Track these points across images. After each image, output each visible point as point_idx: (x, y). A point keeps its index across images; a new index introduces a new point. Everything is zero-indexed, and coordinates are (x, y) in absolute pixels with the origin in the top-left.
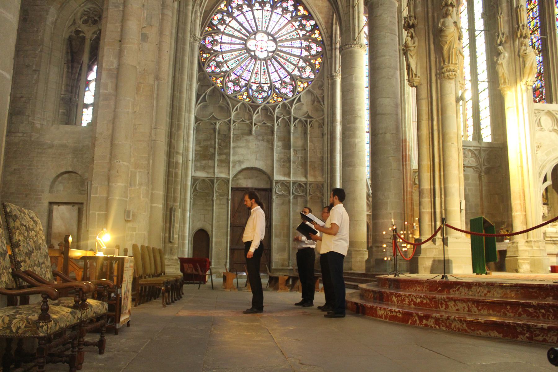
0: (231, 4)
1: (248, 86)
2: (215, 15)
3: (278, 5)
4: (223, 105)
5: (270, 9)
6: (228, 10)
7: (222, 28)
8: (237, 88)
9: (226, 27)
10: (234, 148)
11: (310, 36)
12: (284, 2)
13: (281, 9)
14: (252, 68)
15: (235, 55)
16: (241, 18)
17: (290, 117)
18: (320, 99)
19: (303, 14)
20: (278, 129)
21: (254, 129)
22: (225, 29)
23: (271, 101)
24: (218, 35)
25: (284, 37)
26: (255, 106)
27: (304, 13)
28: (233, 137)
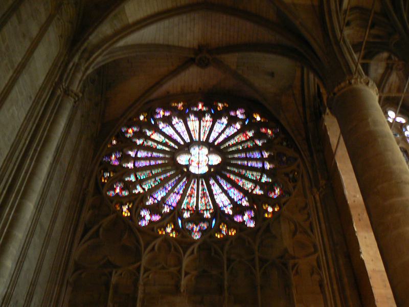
12: (231, 111)
17: (253, 259)
21: (183, 282)
25: (234, 149)
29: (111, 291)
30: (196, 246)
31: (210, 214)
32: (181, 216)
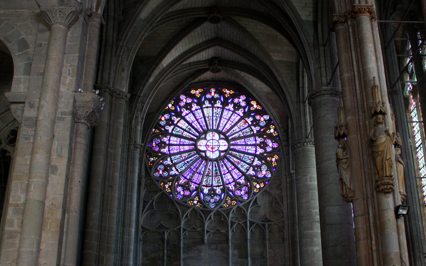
0: (180, 104)
1: (199, 190)
2: (163, 116)
3: (230, 101)
4: (172, 213)
5: (221, 106)
6: (176, 109)
7: (170, 129)
8: (187, 193)
9: (174, 128)
10: (185, 259)
11: (265, 132)
12: (235, 98)
13: (232, 106)
14: (203, 170)
15: (185, 157)
16: (190, 118)
17: (246, 222)
18: (279, 200)
19: (256, 109)
20: (233, 236)
21: (206, 237)
22: (173, 130)
23: (224, 205)
24: (166, 137)
26: (206, 211)
27: (258, 108)
28: (184, 247)
29: (165, 243)
30: (212, 214)
31: (221, 189)
32: (202, 191)
